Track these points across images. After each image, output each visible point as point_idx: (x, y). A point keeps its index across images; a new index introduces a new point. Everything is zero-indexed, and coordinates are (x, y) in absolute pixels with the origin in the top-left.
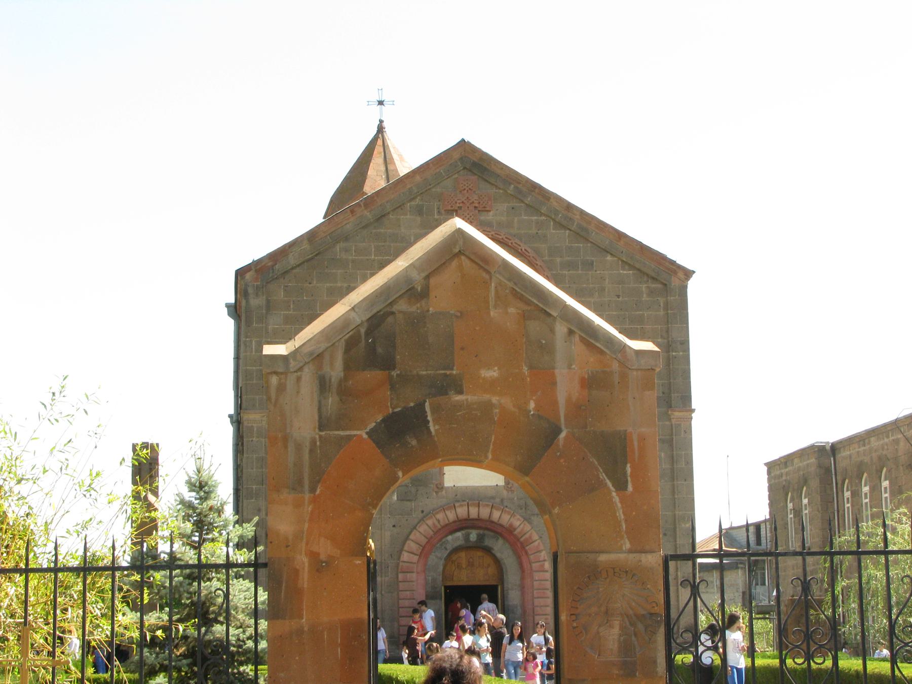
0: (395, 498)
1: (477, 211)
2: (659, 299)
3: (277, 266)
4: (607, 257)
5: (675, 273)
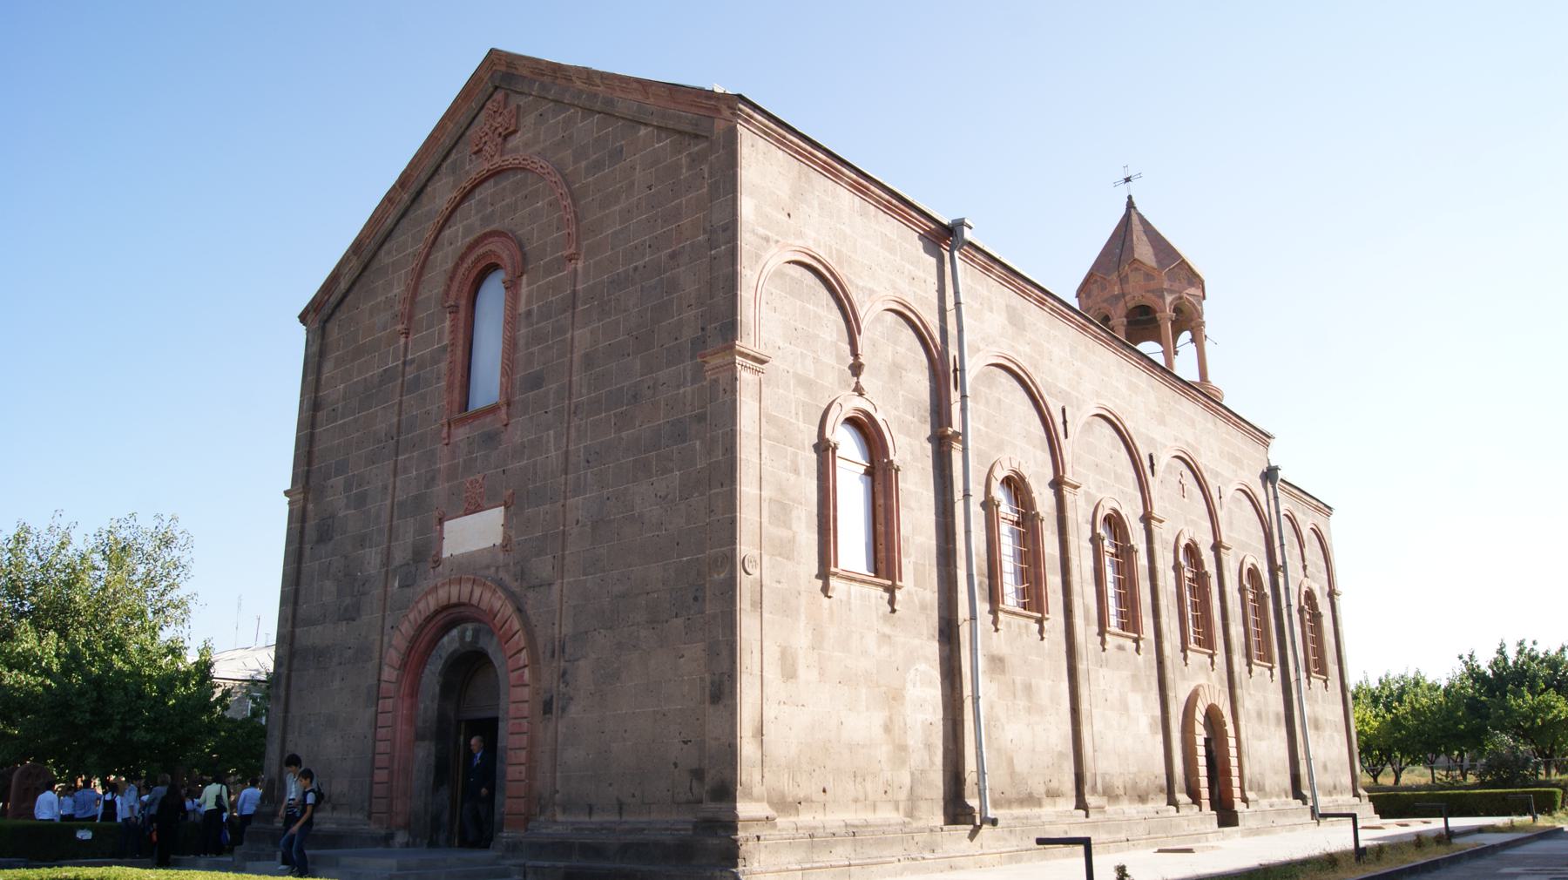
0: (396, 584)
1: (500, 140)
2: (703, 167)
3: (331, 299)
4: (639, 130)
5: (718, 111)
